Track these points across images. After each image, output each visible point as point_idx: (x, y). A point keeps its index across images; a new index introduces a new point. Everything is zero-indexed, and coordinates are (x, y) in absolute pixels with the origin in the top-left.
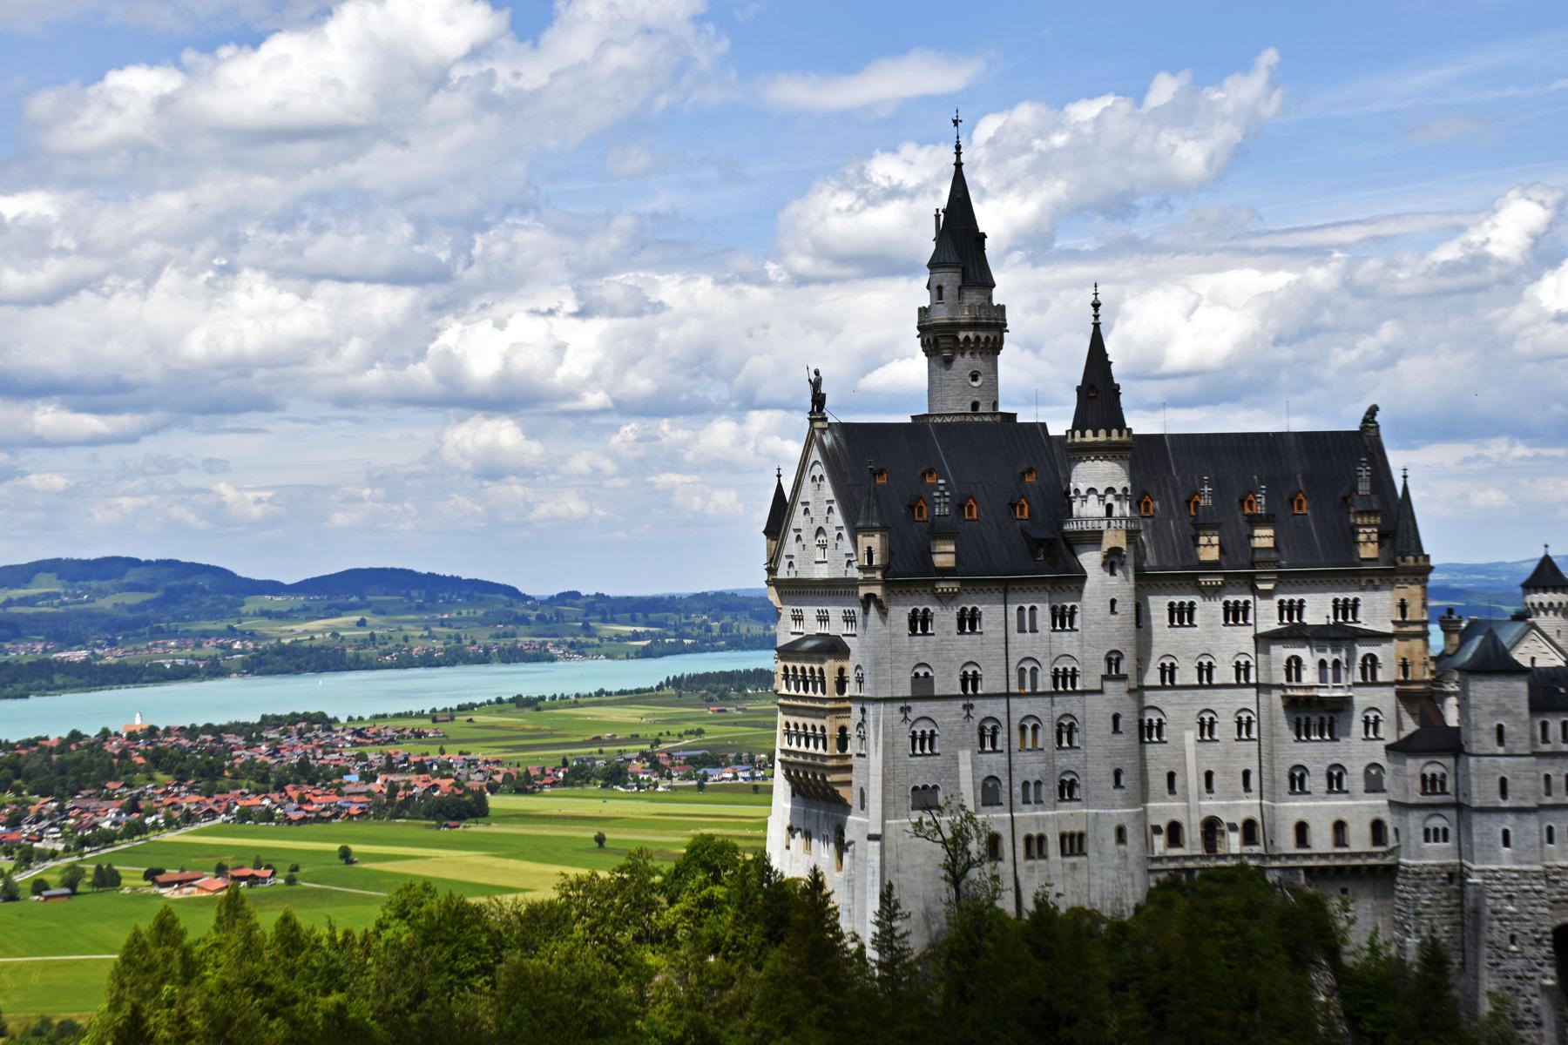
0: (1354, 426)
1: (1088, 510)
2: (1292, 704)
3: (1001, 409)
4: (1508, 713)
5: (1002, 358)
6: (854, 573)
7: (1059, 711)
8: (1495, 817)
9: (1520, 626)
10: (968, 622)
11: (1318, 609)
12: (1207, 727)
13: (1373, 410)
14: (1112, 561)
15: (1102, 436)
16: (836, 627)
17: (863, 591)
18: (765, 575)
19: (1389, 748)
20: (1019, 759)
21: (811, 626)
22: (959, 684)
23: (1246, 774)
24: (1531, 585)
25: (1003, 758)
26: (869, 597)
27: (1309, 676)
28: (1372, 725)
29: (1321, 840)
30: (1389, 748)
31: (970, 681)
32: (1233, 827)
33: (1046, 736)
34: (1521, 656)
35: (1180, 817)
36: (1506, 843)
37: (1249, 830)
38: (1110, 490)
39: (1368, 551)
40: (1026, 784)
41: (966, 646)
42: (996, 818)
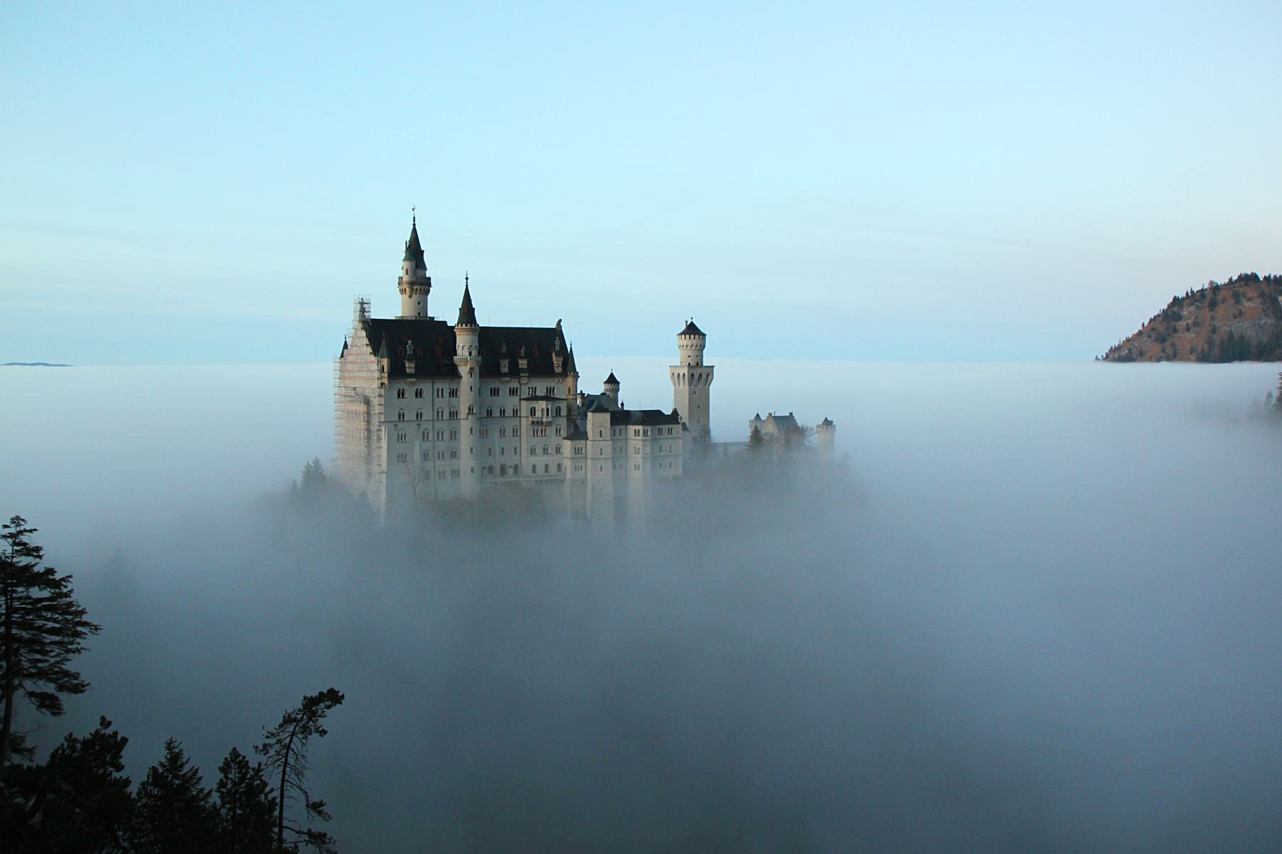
0: (554, 326)
10: (419, 394)
12: (502, 433)
14: (471, 371)
27: (538, 414)
28: (558, 431)
29: (540, 470)
31: (419, 416)
33: (446, 436)
39: (558, 370)
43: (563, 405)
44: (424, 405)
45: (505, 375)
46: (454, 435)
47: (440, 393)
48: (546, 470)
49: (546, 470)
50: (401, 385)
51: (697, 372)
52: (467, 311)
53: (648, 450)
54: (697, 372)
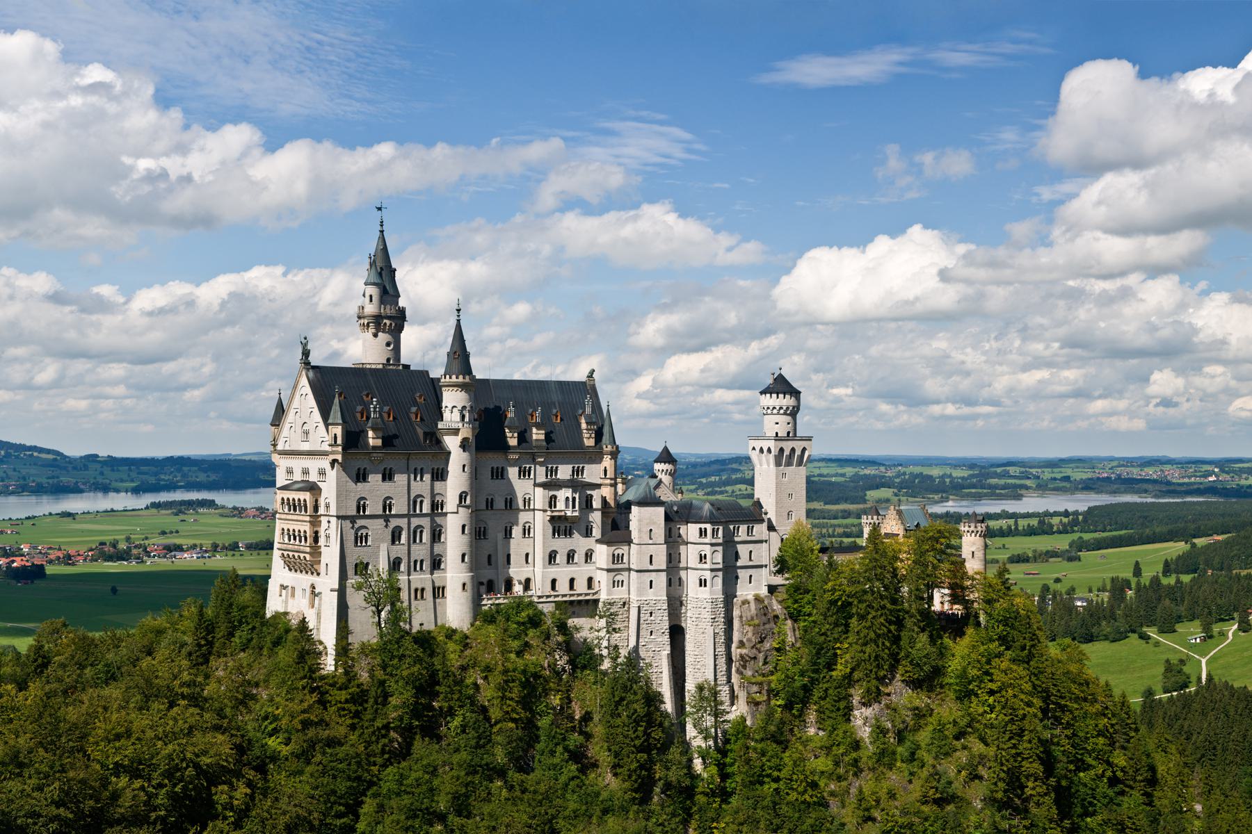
0: (584, 379)
1: (451, 417)
2: (553, 519)
6: (328, 449)
9: (653, 482)
10: (388, 476)
11: (564, 472)
14: (464, 445)
15: (461, 379)
17: (332, 457)
20: (413, 547)
22: (381, 508)
23: (527, 555)
24: (656, 461)
25: (406, 548)
26: (334, 462)
27: (561, 505)
28: (588, 533)
29: (563, 588)
31: (387, 506)
32: (520, 583)
33: (426, 537)
34: (659, 493)
38: (464, 408)
40: (416, 562)
41: (386, 488)
46: (436, 535)
48: (572, 587)
49: (572, 587)
50: (362, 463)
53: (719, 558)
54: (788, 446)
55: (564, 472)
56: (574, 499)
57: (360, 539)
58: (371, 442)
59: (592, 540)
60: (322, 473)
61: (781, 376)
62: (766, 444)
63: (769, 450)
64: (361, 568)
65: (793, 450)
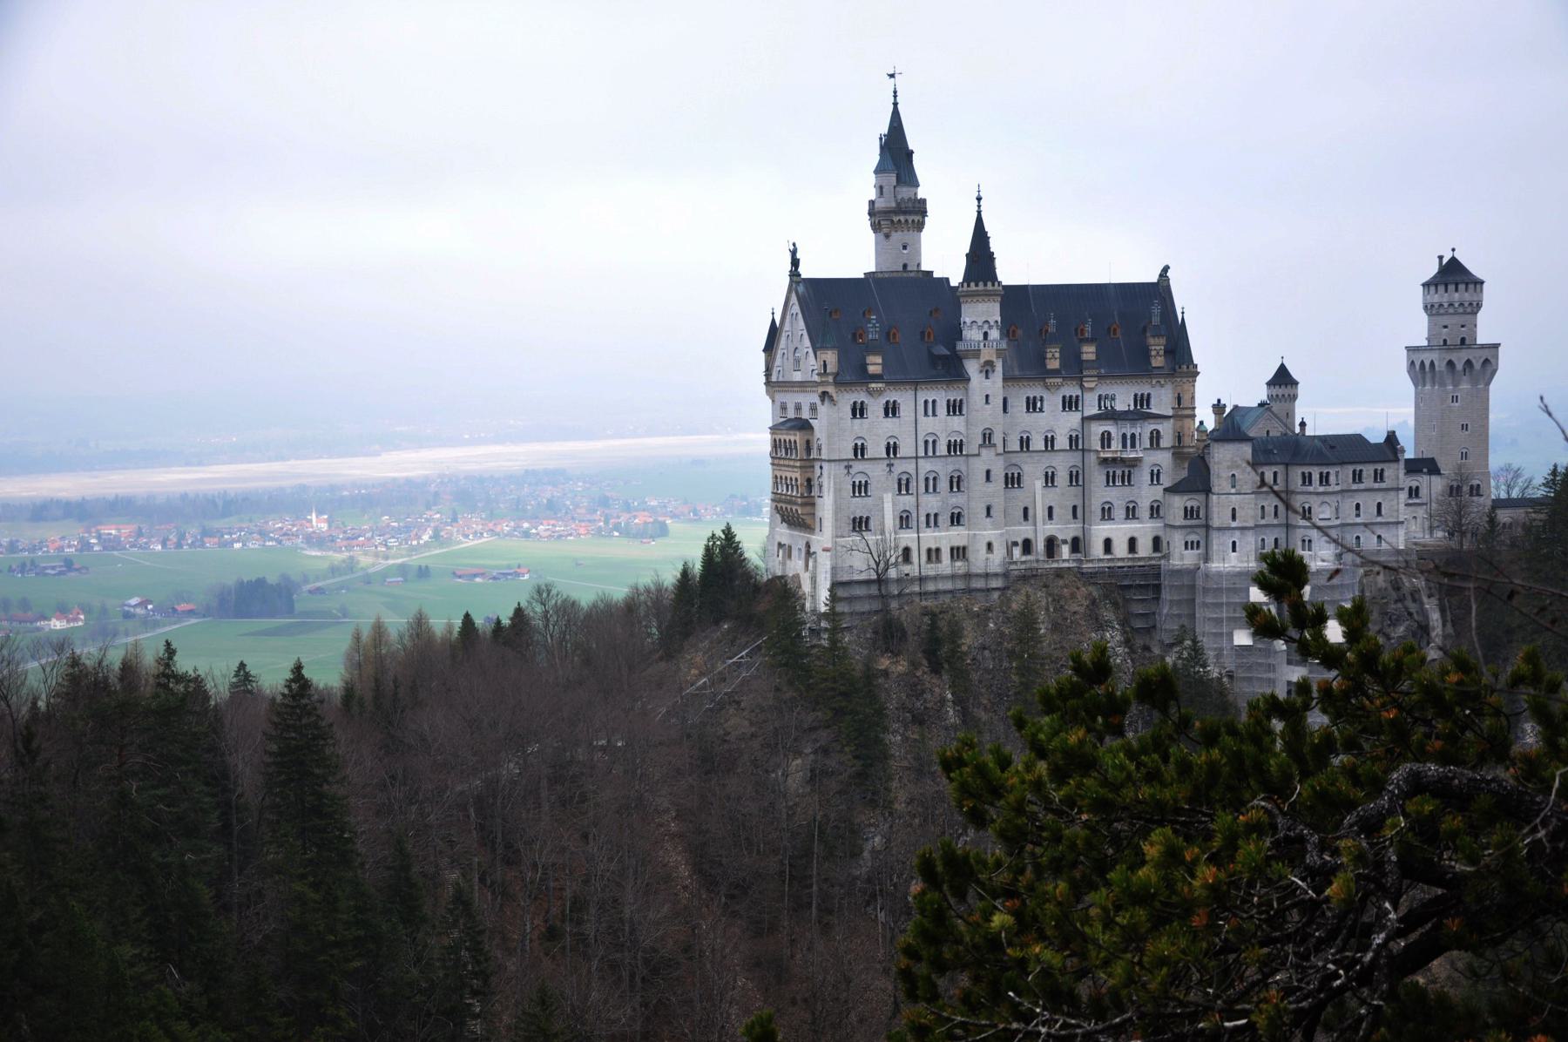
0: (1154, 279)
1: (972, 335)
3: (924, 268)
4: (1238, 467)
5: (926, 235)
6: (816, 378)
7: (951, 468)
8: (1228, 533)
12: (1050, 479)
13: (1166, 269)
14: (987, 370)
16: (805, 415)
17: (821, 389)
18: (763, 379)
19: (1166, 490)
21: (791, 414)
26: (824, 395)
27: (1116, 445)
29: (1120, 550)
30: (1166, 490)
31: (892, 449)
32: (1065, 542)
33: (943, 484)
35: (1030, 536)
36: (1234, 550)
37: (1076, 545)
39: (1158, 361)
40: (928, 516)
42: (908, 538)
43: (1166, 429)
44: (901, 429)
45: (1055, 373)
46: (956, 483)
47: (930, 408)
50: (860, 396)
51: (1459, 359)
52: (980, 256)
54: (1459, 359)
55: (1124, 401)
56: (1133, 436)
57: (861, 489)
58: (872, 369)
59: (1160, 488)
60: (813, 408)
61: (1453, 260)
62: (1427, 358)
63: (1432, 363)
64: (860, 524)
65: (1469, 363)
